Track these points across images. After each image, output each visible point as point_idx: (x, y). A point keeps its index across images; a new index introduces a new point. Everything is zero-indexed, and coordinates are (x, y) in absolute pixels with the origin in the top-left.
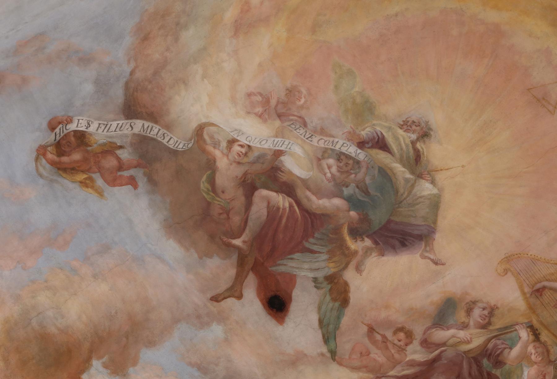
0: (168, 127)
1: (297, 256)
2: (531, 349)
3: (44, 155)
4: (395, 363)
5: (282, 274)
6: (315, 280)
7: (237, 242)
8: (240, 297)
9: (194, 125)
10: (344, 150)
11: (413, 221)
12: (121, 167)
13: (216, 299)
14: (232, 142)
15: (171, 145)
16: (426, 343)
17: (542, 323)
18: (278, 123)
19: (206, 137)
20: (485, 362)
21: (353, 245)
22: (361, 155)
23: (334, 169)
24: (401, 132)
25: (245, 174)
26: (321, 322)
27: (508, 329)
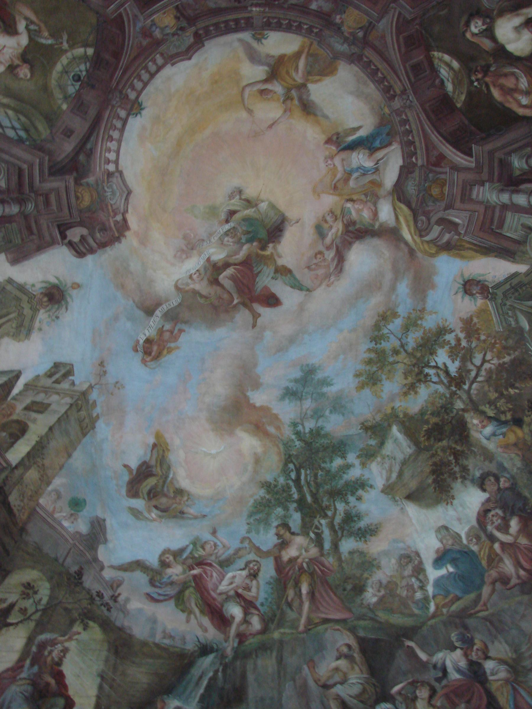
0: (167, 300)
1: (257, 279)
2: (356, 206)
3: (146, 361)
4: (328, 266)
5: (261, 291)
6: (273, 278)
7: (236, 301)
8: (259, 315)
9: (173, 289)
10: (225, 230)
11: (274, 220)
12: (172, 332)
13: (254, 326)
14: (191, 277)
15: (175, 304)
16: (328, 248)
17: (348, 195)
18: (195, 252)
19: (181, 287)
20: (351, 228)
21: (268, 252)
22: (231, 224)
23: (231, 240)
24: (233, 201)
25: (208, 280)
26: (292, 287)
27: (343, 210)
